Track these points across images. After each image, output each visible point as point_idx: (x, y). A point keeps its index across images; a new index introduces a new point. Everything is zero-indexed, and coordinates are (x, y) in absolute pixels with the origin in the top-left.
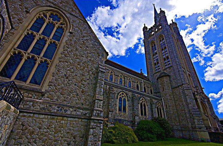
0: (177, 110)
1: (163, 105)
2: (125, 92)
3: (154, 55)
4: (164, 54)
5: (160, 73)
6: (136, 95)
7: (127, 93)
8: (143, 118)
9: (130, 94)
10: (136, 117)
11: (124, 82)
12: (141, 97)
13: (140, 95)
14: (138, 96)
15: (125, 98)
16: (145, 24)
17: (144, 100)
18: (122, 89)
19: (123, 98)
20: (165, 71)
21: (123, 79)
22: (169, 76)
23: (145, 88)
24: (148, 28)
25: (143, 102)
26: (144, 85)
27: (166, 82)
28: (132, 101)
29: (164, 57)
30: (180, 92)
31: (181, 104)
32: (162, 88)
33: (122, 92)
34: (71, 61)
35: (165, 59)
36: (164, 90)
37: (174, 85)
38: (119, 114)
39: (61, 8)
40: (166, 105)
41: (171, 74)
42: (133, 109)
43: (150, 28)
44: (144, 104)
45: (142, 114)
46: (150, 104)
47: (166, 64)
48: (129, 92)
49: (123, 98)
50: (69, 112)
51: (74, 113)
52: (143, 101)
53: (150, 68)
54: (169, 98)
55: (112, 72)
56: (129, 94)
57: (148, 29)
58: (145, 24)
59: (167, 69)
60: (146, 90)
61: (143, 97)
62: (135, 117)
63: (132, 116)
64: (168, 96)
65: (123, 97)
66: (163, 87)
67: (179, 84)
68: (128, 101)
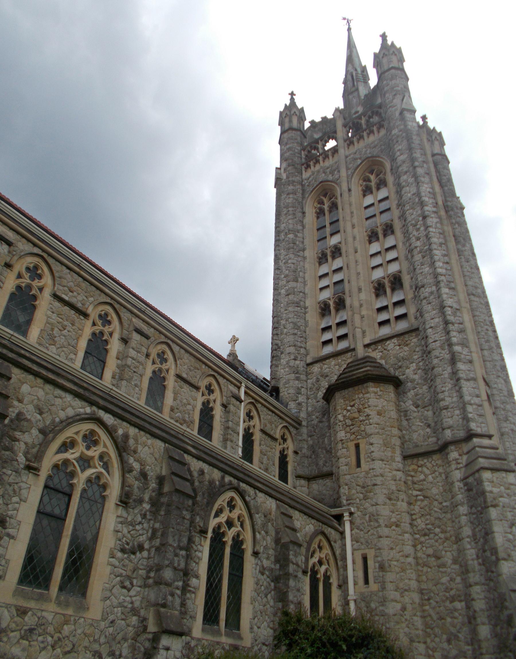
0: (421, 592)
1: (344, 558)
3: (322, 259)
4: (377, 261)
5: (348, 358)
7: (126, 436)
10: (165, 641)
11: (122, 368)
12: (223, 488)
13: (217, 474)
14: (202, 472)
15: (98, 477)
17: (240, 509)
18: (92, 403)
19: (90, 472)
20: (376, 354)
22: (397, 383)
23: (248, 437)
25: (230, 524)
26: (249, 416)
27: (379, 414)
28: (155, 503)
29: (378, 274)
30: (449, 484)
31: (448, 558)
32: (353, 449)
33: (86, 427)
35: (379, 289)
36: (359, 465)
37: (421, 436)
38: (22, 612)
40: (365, 559)
41: (411, 373)
42: (154, 578)
43: (318, 119)
44: (238, 543)
45: (211, 617)
46: (277, 541)
47: (383, 316)
48: (144, 437)
49: (81, 479)
52: (235, 515)
53: (296, 326)
54: (385, 511)
56: (144, 452)
59: (390, 345)
60: (257, 448)
61: (237, 490)
62: (156, 639)
63: (137, 635)
64: (381, 498)
65: (85, 462)
66: (357, 446)
67: (448, 434)
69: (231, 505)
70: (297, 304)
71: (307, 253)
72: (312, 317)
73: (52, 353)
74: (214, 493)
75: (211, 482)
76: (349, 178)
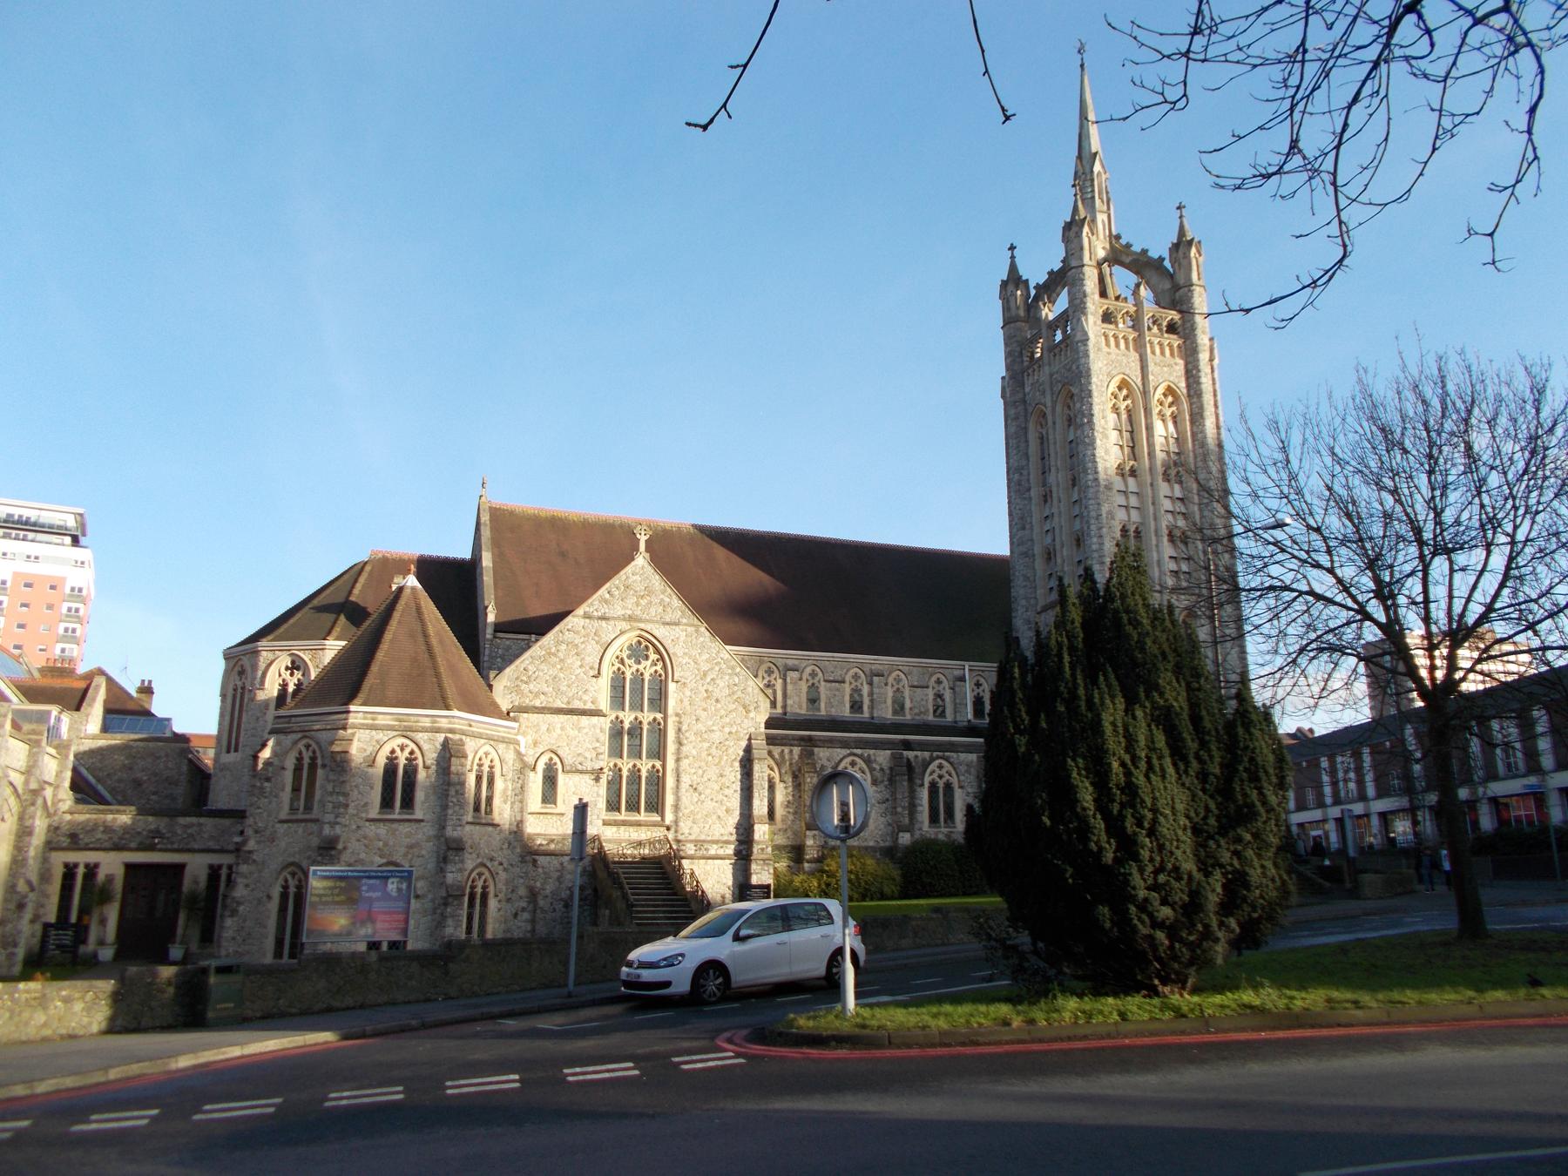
2: (860, 756)
6: (910, 754)
8: (941, 833)
9: (883, 757)
11: (872, 701)
12: (932, 759)
13: (927, 754)
16: (1012, 248)
21: (866, 689)
24: (1032, 285)
26: (978, 685)
28: (890, 780)
34: (694, 752)
39: (640, 620)
43: (1042, 278)
50: (712, 852)
51: (721, 852)
52: (943, 772)
53: (1027, 578)
55: (813, 674)
57: (1033, 292)
58: (1012, 248)
68: (875, 782)
69: (940, 767)
70: (1025, 554)
71: (1033, 493)
72: (1039, 564)
73: (833, 712)
74: (926, 764)
75: (924, 760)
76: (1054, 403)
